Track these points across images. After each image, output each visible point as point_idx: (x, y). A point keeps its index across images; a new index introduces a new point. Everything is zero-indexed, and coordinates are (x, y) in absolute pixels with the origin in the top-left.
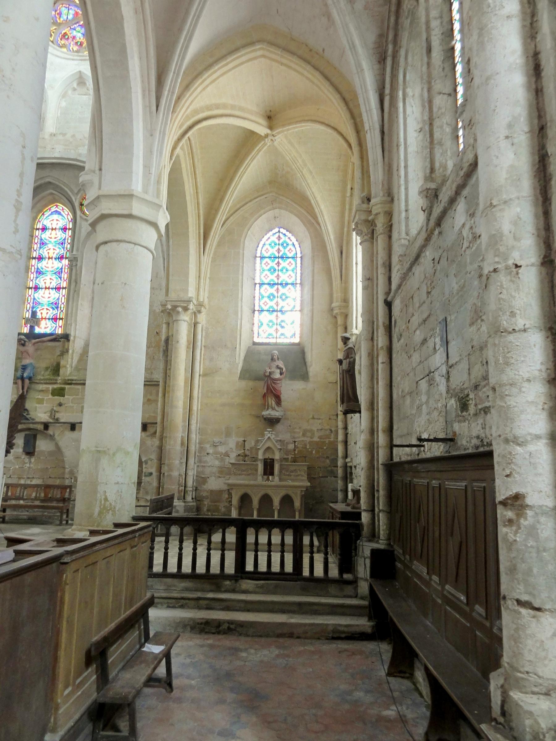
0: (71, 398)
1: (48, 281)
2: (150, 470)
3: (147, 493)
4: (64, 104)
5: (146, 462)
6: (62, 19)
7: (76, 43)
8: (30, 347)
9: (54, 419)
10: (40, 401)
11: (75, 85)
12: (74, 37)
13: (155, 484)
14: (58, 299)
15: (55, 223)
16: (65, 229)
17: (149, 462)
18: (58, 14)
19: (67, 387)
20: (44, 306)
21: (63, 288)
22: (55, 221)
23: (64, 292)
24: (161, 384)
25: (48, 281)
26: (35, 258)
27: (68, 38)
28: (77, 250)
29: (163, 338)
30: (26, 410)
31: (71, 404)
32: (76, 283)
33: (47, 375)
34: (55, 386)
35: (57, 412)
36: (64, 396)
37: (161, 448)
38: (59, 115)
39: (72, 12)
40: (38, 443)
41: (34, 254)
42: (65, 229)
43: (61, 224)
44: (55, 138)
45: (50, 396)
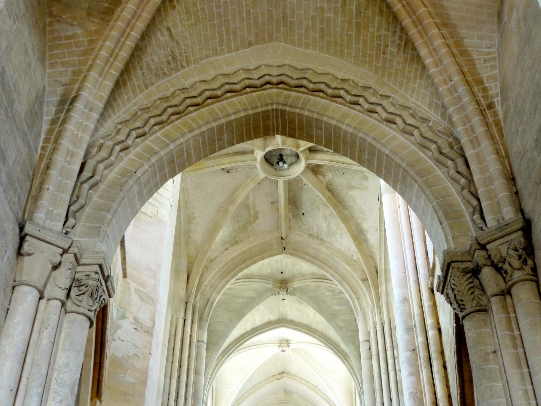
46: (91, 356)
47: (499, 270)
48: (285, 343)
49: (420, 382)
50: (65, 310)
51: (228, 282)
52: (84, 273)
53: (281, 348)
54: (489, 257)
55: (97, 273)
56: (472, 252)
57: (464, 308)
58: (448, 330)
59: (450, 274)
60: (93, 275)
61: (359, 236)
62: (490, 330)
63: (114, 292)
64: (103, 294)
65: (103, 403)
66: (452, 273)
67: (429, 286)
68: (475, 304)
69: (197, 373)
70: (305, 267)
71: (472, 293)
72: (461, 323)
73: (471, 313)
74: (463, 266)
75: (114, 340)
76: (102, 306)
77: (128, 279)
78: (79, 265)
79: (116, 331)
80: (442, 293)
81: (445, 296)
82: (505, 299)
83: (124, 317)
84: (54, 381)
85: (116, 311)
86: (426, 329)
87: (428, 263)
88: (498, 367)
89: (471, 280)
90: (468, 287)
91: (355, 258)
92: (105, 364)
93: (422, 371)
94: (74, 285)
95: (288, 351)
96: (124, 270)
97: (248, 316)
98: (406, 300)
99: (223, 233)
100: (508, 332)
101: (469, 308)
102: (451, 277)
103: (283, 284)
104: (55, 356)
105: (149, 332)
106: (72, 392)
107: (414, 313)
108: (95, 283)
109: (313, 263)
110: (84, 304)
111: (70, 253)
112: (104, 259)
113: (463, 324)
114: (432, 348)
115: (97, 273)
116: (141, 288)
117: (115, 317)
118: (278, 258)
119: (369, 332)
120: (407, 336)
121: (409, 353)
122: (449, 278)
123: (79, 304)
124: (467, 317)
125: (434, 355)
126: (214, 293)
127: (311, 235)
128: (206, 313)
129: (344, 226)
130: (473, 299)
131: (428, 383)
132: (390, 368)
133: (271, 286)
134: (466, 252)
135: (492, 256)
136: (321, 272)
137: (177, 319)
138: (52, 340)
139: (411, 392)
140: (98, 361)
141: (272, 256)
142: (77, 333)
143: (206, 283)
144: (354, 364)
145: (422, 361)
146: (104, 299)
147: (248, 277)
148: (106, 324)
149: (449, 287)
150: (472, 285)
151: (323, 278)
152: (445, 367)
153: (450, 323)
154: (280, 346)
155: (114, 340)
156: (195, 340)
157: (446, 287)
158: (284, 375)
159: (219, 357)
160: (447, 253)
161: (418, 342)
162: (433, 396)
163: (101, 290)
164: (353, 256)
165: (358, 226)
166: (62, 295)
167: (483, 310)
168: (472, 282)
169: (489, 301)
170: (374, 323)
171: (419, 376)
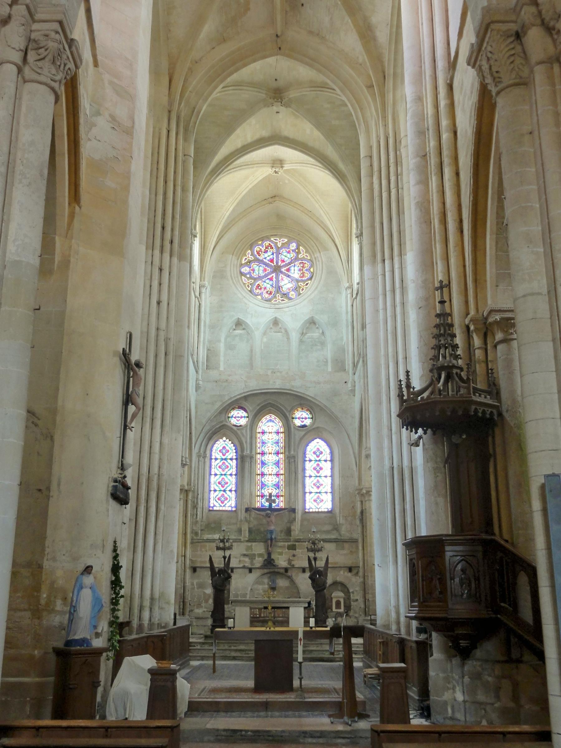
0: (300, 551)
1: (270, 470)
2: (356, 598)
3: (355, 612)
4: (265, 340)
5: (353, 593)
6: (255, 274)
7: (267, 292)
8: (273, 518)
9: (290, 565)
10: (281, 554)
11: (271, 326)
12: (265, 288)
13: (363, 606)
14: (279, 482)
15: (270, 428)
16: (278, 433)
17: (355, 593)
18: (252, 270)
19: (297, 543)
20: (269, 487)
21: (281, 475)
22: (270, 427)
23: (282, 477)
24: (360, 540)
25: (270, 470)
26: (259, 453)
27: (261, 289)
28: (294, 451)
29: (359, 511)
30: (273, 560)
31: (301, 555)
32: (296, 473)
33: (283, 536)
34: (289, 543)
35: (293, 560)
36: (295, 550)
37: (364, 583)
38: (263, 348)
39: (261, 268)
40: (277, 581)
41: (259, 451)
42: (278, 433)
43: (275, 429)
44: (275, 375)
45: (287, 550)
46: (64, 154)
47: (549, 30)
48: (278, 163)
49: (429, 191)
50: (23, 78)
51: (216, 88)
52: (43, 32)
53: (274, 169)
54: (540, 12)
55: (57, 32)
56: (518, 8)
57: (500, 82)
58: (466, 131)
59: (487, 39)
60: (53, 34)
61: (366, 33)
62: (527, 107)
63: (81, 64)
64: (67, 62)
65: (82, 208)
66: (490, 38)
67: (448, 82)
68: (513, 76)
69: (184, 190)
70: (304, 72)
71: (512, 62)
72: (493, 102)
73: (508, 87)
74: (504, 27)
75: (89, 140)
76: (68, 78)
77: (100, 69)
78: (34, 21)
79: (91, 129)
80: (473, 67)
81: (476, 71)
82: (552, 68)
83: (98, 113)
84: (18, 162)
85: (89, 105)
86: (439, 132)
87: (449, 54)
88: (532, 150)
89: (512, 46)
90: (508, 54)
91: (361, 61)
92: (81, 165)
93: (432, 180)
94: (30, 47)
95: (281, 171)
96: (95, 56)
97: (238, 131)
98: (419, 99)
99: (209, 28)
100: (551, 108)
101: (507, 80)
102: (488, 43)
103: (277, 94)
104: (17, 132)
105: (129, 132)
106: (41, 175)
107: (427, 114)
108: (56, 45)
109: (311, 66)
110: (45, 71)
111: (22, 4)
112: (64, 14)
113: (495, 103)
114: (445, 153)
115: (57, 32)
116: (115, 80)
117: (88, 113)
118: (271, 60)
119: (371, 147)
120: (418, 141)
121: (418, 159)
122: (485, 45)
123: (39, 71)
124: (503, 93)
125: (446, 160)
126: (201, 101)
127: (311, 32)
128: (191, 124)
129: (350, 21)
130: (513, 69)
131: (438, 192)
132: (392, 185)
133: (264, 95)
134: (511, 9)
135: (543, 12)
136: (320, 78)
137: (160, 129)
138: (11, 112)
139: (418, 202)
140: (73, 162)
141: (265, 57)
142: (40, 106)
143: (190, 89)
144: (353, 185)
145: (433, 167)
146: (69, 69)
147: (238, 84)
148: (78, 118)
149: (484, 56)
150: (513, 52)
151: (323, 86)
152: (458, 174)
153: (470, 120)
154: (273, 167)
155: (89, 140)
156: (180, 154)
157: (479, 58)
158: (277, 198)
159: (207, 177)
160: (487, 11)
161: (429, 147)
162: (441, 205)
163: (64, 57)
164: (358, 58)
165: (366, 19)
166: (17, 57)
167: (524, 83)
168: (513, 48)
169: (532, 71)
170: (378, 137)
171: (428, 185)
